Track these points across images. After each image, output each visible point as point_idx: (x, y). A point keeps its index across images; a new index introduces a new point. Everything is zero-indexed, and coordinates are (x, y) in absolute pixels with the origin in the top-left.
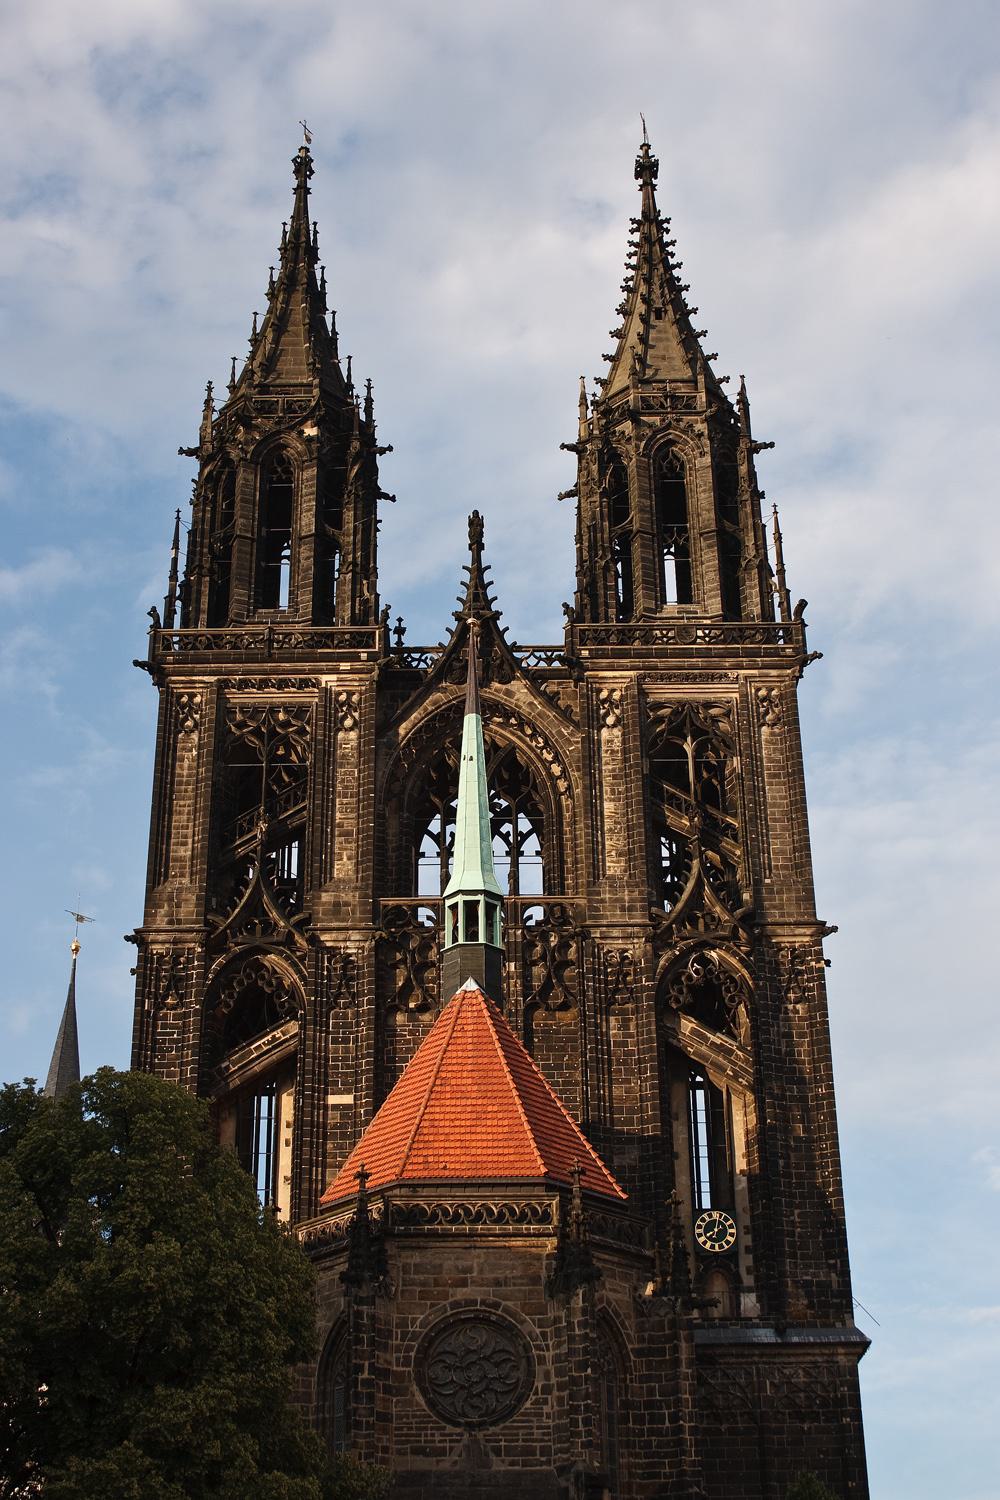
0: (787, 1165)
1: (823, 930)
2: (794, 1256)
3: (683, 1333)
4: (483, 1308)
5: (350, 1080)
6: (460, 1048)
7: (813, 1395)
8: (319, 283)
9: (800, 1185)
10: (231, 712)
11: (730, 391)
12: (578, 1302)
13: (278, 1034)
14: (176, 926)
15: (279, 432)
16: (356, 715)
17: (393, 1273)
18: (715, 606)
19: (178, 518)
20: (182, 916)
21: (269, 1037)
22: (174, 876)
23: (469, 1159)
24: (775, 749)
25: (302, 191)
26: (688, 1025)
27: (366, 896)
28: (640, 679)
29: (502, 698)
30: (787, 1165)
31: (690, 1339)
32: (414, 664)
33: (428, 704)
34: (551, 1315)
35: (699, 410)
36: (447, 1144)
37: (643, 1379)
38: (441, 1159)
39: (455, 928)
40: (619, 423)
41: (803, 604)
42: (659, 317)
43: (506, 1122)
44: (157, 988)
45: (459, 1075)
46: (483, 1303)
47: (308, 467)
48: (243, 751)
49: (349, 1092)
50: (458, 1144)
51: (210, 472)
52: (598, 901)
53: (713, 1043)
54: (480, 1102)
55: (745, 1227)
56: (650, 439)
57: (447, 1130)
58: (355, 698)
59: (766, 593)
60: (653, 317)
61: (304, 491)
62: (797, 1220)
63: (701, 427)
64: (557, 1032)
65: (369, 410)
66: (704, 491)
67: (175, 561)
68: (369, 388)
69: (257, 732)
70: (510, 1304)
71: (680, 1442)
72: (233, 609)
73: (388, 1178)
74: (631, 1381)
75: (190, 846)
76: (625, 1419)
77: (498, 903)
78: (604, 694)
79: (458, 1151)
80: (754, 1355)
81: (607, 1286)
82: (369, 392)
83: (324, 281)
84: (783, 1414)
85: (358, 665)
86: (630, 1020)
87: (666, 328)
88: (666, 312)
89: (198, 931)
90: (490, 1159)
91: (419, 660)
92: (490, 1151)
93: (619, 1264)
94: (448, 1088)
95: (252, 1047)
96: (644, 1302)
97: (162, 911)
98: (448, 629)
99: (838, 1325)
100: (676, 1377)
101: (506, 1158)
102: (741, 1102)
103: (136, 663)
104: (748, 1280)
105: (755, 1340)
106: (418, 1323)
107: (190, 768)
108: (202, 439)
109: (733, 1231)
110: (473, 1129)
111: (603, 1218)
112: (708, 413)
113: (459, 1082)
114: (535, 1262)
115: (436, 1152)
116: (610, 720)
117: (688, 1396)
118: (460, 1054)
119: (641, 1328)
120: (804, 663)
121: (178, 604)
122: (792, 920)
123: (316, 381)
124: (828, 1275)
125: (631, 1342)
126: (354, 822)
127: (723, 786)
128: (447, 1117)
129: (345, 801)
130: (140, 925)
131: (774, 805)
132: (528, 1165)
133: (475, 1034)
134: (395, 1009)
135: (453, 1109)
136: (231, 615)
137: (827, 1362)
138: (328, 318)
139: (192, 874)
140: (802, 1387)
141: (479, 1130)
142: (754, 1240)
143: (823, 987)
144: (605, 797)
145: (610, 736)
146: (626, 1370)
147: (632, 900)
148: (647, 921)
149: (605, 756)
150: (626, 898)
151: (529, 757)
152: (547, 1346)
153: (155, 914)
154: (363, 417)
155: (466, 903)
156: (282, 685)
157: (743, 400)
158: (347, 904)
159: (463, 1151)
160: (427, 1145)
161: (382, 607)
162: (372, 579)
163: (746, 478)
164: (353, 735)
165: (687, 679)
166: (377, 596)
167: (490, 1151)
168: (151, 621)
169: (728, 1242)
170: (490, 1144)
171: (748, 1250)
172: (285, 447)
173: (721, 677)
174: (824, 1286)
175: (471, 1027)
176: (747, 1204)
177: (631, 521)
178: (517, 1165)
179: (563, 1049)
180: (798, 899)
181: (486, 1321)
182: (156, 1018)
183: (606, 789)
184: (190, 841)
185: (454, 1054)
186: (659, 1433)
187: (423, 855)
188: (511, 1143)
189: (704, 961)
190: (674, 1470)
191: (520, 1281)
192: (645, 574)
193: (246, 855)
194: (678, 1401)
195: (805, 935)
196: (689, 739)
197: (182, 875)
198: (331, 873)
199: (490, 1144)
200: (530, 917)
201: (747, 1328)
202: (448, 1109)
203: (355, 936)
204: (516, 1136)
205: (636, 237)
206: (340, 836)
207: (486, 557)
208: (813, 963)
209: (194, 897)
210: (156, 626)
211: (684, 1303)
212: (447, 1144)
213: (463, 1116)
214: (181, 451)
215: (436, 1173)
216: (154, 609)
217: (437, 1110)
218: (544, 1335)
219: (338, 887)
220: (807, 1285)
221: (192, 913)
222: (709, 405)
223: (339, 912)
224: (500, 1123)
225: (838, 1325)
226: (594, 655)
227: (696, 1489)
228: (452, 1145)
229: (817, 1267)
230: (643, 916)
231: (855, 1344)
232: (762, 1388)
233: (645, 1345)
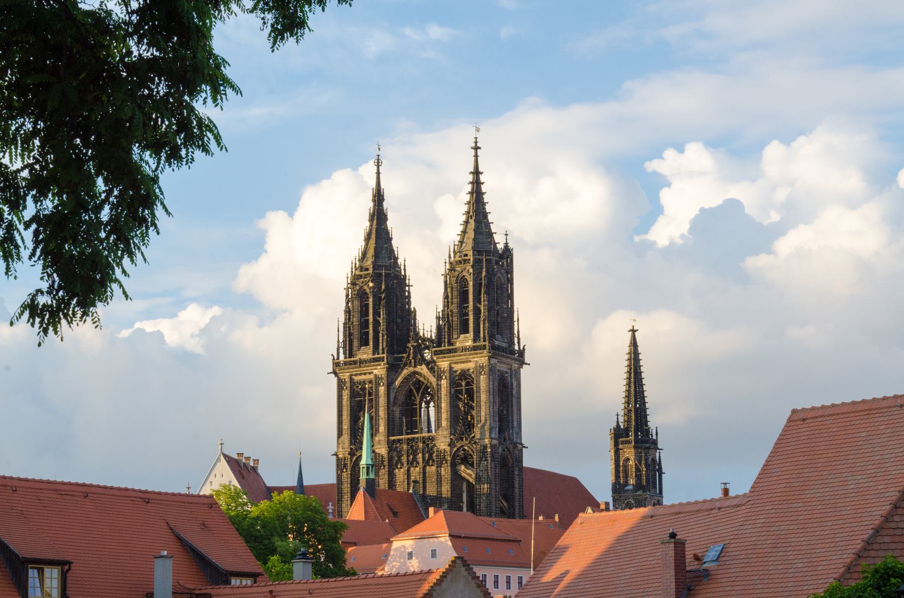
0: (480, 507)
9: (483, 512)
20: (345, 447)
26: (463, 467)
28: (451, 363)
29: (420, 371)
30: (480, 507)
48: (359, 395)
69: (361, 389)
85: (381, 367)
97: (341, 446)
121: (341, 350)
134: (394, 469)
145: (444, 383)
149: (443, 389)
156: (365, 374)
164: (383, 388)
165: (461, 362)
183: (442, 399)
210: (334, 359)
226: (438, 358)
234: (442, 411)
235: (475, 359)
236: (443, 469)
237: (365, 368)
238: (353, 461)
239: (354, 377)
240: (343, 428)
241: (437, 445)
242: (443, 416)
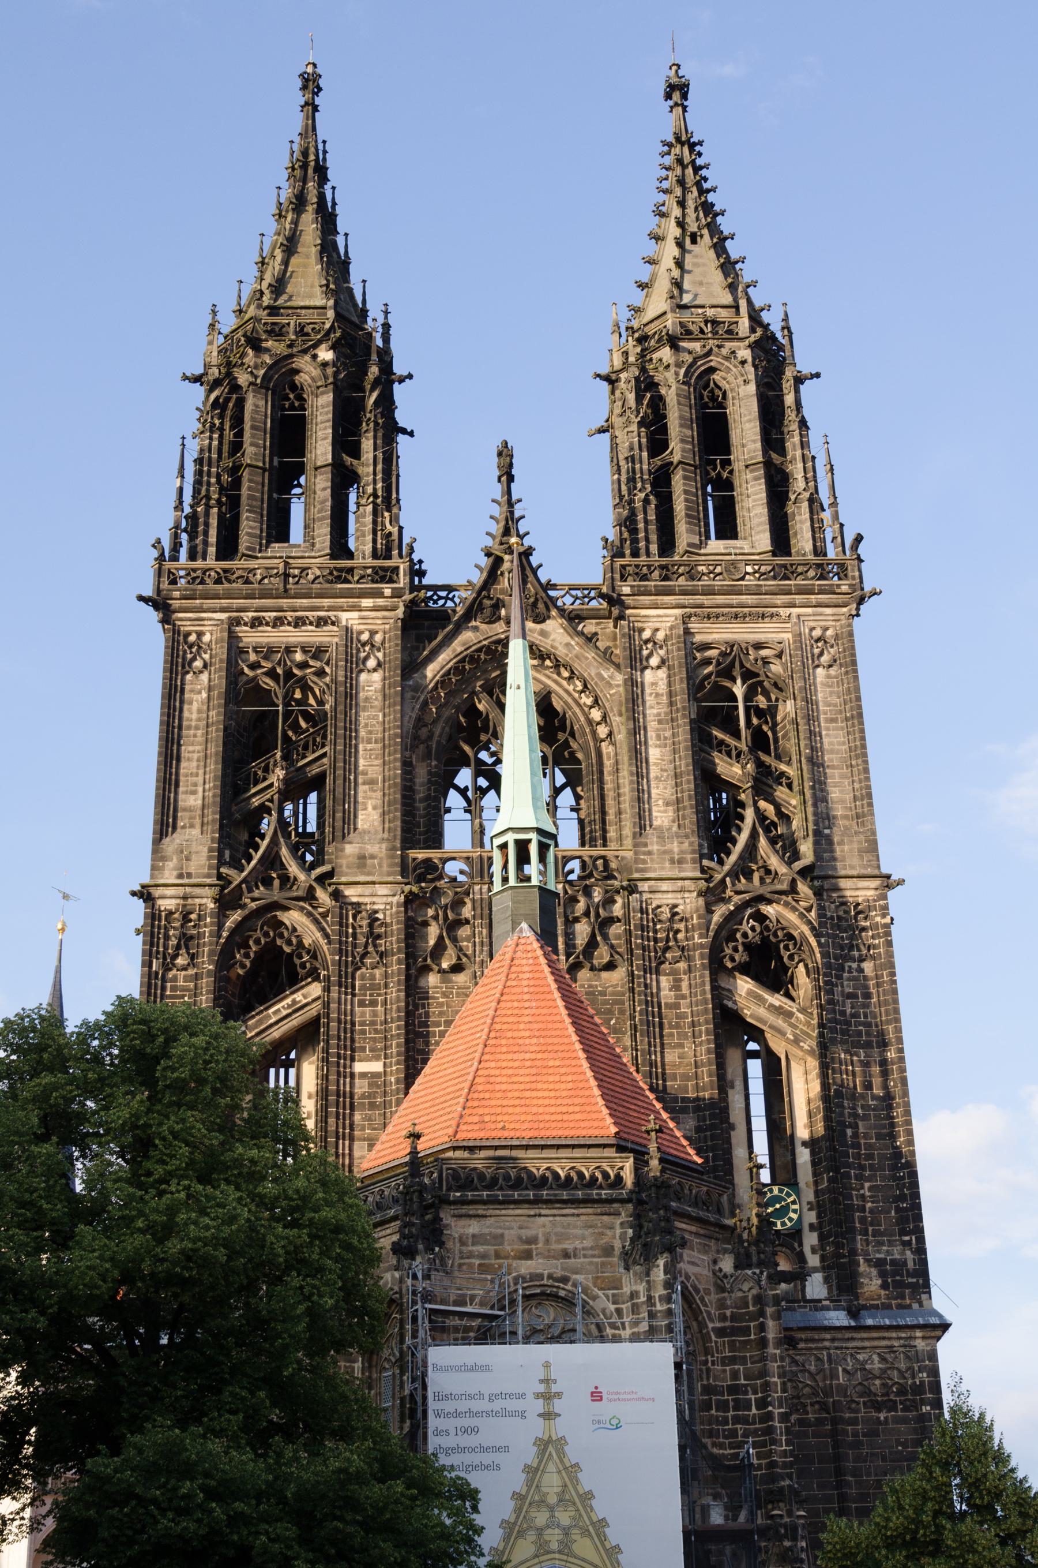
0: (856, 1135)
1: (888, 883)
2: (865, 1233)
3: (769, 1310)
4: (550, 1283)
5: (379, 1045)
6: (515, 997)
7: (890, 1382)
8: (330, 204)
9: (870, 1157)
10: (243, 651)
11: (773, 319)
12: (659, 1274)
13: (298, 997)
14: (186, 881)
15: (291, 356)
16: (380, 655)
17: (449, 1245)
18: (763, 541)
19: (183, 445)
20: (192, 870)
21: (289, 1001)
22: (183, 827)
23: (530, 1118)
24: (831, 693)
25: (311, 108)
26: (744, 985)
27: (393, 849)
28: (686, 619)
30: (856, 1135)
31: (777, 1317)
32: (441, 602)
33: (457, 646)
34: (626, 1290)
35: (741, 335)
36: (505, 1102)
37: (724, 1362)
38: (499, 1118)
39: (505, 867)
40: (656, 349)
41: (859, 539)
42: (694, 241)
43: (569, 1078)
44: (166, 947)
45: (515, 1027)
46: (550, 1277)
47: (323, 393)
49: (377, 1058)
50: (517, 1102)
51: (217, 398)
52: (644, 854)
53: (771, 1005)
54: (539, 1056)
55: (809, 1203)
56: (691, 366)
57: (504, 1087)
58: (378, 638)
59: (817, 528)
60: (688, 240)
61: (319, 418)
62: (868, 1194)
63: (745, 354)
64: (603, 994)
65: (386, 337)
66: (750, 421)
67: (181, 490)
68: (386, 313)
70: (579, 1278)
71: (770, 1431)
72: (244, 542)
73: (440, 1141)
74: (713, 1363)
75: (200, 794)
76: (707, 1406)
77: (552, 843)
78: (646, 635)
79: (518, 1110)
80: (824, 1340)
81: (686, 1258)
82: (386, 318)
83: (334, 204)
84: (858, 1403)
85: (380, 602)
86: (680, 980)
87: (702, 253)
88: (702, 236)
89: (210, 886)
90: (553, 1118)
91: (447, 598)
92: (552, 1110)
93: (697, 1234)
94: (504, 1042)
95: (271, 1011)
96: (725, 1276)
97: (170, 865)
98: (477, 566)
99: (915, 1306)
100: (763, 1359)
101: (572, 1117)
102: (802, 1069)
103: (141, 598)
104: (813, 1260)
105: (826, 1323)
106: (477, 1300)
107: (199, 711)
108: (207, 366)
109: (796, 1207)
110: (533, 1086)
111: (679, 1183)
112: (753, 339)
113: (516, 1034)
114: (609, 1232)
115: (493, 1111)
116: (654, 661)
117: (776, 1379)
118: (516, 1004)
119: (722, 1305)
120: (861, 601)
121: (184, 537)
122: (854, 873)
123: (331, 303)
124: (903, 1253)
125: (712, 1320)
126: (380, 769)
127: (775, 733)
128: (504, 1072)
129: (369, 746)
130: (146, 880)
131: (832, 752)
132: (596, 1124)
133: (532, 983)
134: (426, 969)
135: (511, 1064)
136: (242, 548)
137: (904, 1346)
138: (340, 240)
139: (203, 824)
140: (877, 1373)
141: (539, 1086)
142: (819, 1217)
143: (889, 944)
144: (650, 742)
146: (707, 1351)
147: (682, 852)
148: (698, 874)
149: (650, 700)
150: (676, 850)
151: (566, 703)
152: (623, 1324)
153: (163, 868)
154: (379, 342)
155: (517, 842)
157: (786, 328)
158: (373, 857)
159: (524, 1109)
160: (483, 1103)
161: (406, 540)
162: (395, 510)
163: (794, 407)
164: (377, 677)
166: (401, 528)
167: (552, 1110)
168: (155, 554)
169: (791, 1219)
170: (553, 1102)
171: (812, 1227)
172: (297, 372)
173: (772, 616)
174: (899, 1265)
175: (528, 975)
176: (810, 1178)
177: (671, 453)
178: (583, 1124)
179: (610, 1012)
180: (860, 851)
181: (555, 1297)
182: (164, 980)
183: (651, 734)
184: (200, 789)
185: (509, 1005)
186: (745, 1421)
187: (448, 810)
188: (577, 1101)
189: (760, 917)
190: (763, 1462)
191: (590, 1252)
192: (688, 508)
193: (262, 805)
194: (766, 1386)
195: (868, 889)
196: (739, 681)
197: (192, 826)
198: (355, 824)
199: (553, 1102)
200: (572, 871)
201: (816, 1310)
202: (504, 1064)
203: (382, 890)
204: (581, 1093)
205: (668, 160)
206: (364, 784)
207: (516, 489)
208: (878, 919)
209: (206, 849)
210: (161, 558)
211: (770, 1277)
212: (505, 1102)
213: (522, 1071)
214: (185, 378)
215: (494, 1134)
216: (159, 541)
217: (493, 1065)
218: (619, 1312)
219: (362, 838)
220: (879, 1264)
221: (202, 867)
222: (753, 330)
223: (364, 865)
224: (563, 1078)
225: (915, 1306)
226: (637, 592)
227: (787, 1482)
228: (511, 1102)
229: (891, 1243)
230: (695, 868)
231: (934, 1327)
232: (834, 1375)
233: (728, 1324)
234: (652, 775)
235: (795, 611)
236: (665, 982)
237: (305, 602)
238: (229, 924)
239: (242, 630)
240: (181, 804)
241: (644, 886)
242: (654, 791)
